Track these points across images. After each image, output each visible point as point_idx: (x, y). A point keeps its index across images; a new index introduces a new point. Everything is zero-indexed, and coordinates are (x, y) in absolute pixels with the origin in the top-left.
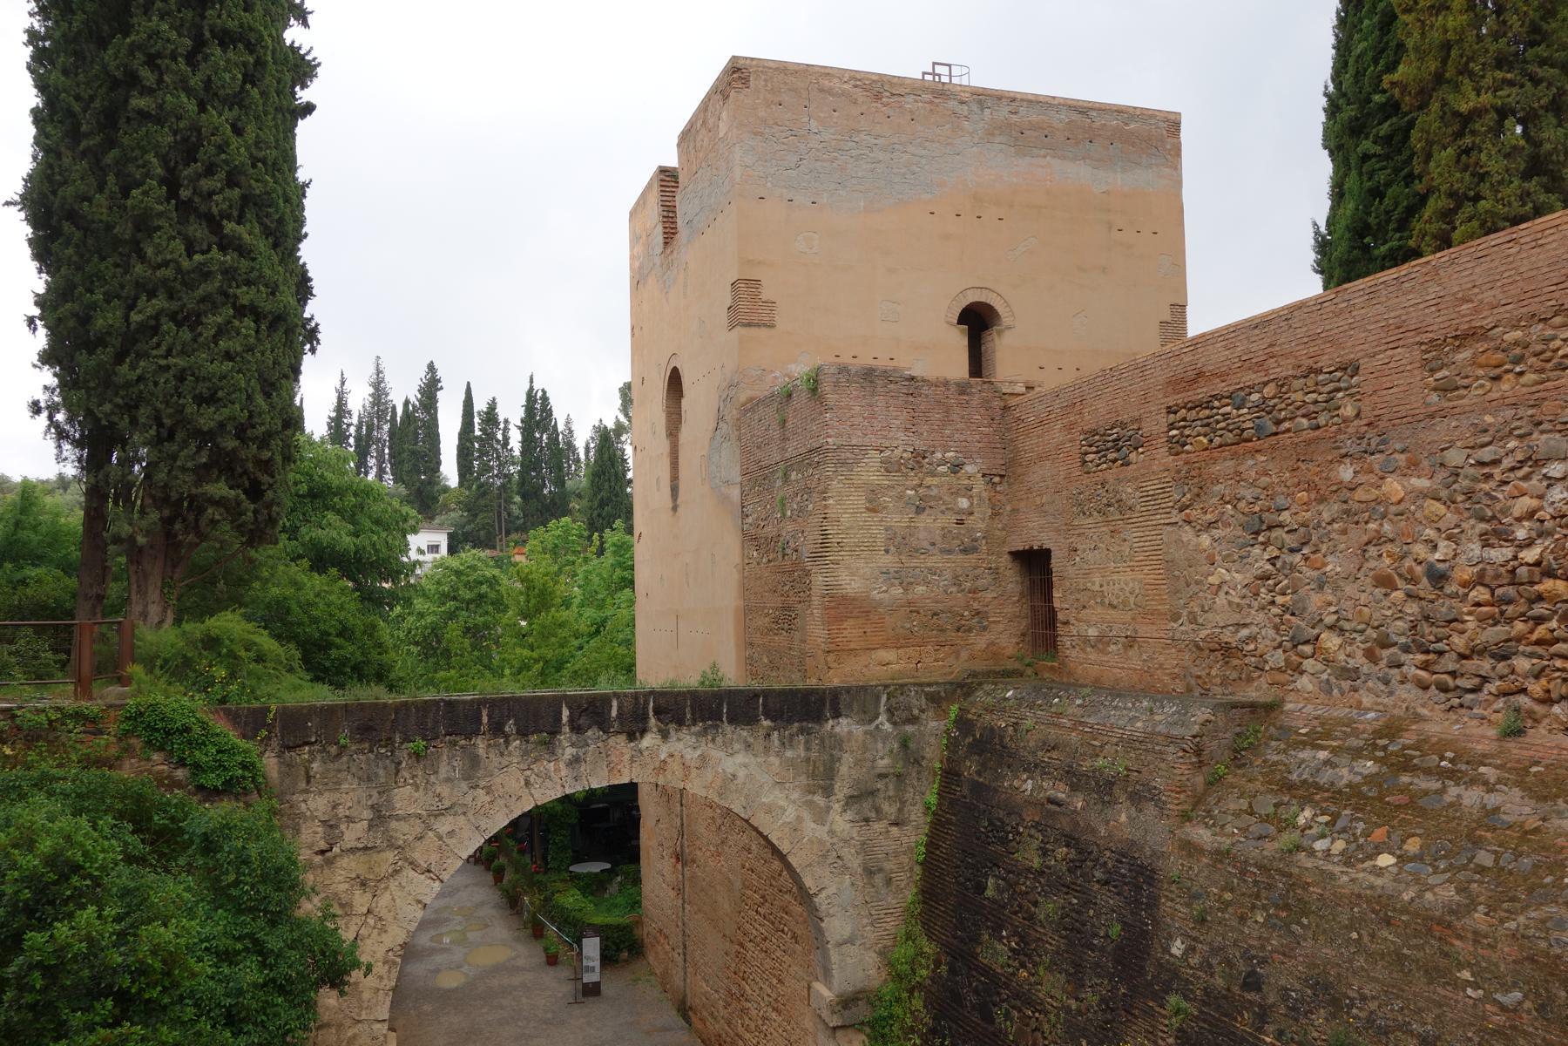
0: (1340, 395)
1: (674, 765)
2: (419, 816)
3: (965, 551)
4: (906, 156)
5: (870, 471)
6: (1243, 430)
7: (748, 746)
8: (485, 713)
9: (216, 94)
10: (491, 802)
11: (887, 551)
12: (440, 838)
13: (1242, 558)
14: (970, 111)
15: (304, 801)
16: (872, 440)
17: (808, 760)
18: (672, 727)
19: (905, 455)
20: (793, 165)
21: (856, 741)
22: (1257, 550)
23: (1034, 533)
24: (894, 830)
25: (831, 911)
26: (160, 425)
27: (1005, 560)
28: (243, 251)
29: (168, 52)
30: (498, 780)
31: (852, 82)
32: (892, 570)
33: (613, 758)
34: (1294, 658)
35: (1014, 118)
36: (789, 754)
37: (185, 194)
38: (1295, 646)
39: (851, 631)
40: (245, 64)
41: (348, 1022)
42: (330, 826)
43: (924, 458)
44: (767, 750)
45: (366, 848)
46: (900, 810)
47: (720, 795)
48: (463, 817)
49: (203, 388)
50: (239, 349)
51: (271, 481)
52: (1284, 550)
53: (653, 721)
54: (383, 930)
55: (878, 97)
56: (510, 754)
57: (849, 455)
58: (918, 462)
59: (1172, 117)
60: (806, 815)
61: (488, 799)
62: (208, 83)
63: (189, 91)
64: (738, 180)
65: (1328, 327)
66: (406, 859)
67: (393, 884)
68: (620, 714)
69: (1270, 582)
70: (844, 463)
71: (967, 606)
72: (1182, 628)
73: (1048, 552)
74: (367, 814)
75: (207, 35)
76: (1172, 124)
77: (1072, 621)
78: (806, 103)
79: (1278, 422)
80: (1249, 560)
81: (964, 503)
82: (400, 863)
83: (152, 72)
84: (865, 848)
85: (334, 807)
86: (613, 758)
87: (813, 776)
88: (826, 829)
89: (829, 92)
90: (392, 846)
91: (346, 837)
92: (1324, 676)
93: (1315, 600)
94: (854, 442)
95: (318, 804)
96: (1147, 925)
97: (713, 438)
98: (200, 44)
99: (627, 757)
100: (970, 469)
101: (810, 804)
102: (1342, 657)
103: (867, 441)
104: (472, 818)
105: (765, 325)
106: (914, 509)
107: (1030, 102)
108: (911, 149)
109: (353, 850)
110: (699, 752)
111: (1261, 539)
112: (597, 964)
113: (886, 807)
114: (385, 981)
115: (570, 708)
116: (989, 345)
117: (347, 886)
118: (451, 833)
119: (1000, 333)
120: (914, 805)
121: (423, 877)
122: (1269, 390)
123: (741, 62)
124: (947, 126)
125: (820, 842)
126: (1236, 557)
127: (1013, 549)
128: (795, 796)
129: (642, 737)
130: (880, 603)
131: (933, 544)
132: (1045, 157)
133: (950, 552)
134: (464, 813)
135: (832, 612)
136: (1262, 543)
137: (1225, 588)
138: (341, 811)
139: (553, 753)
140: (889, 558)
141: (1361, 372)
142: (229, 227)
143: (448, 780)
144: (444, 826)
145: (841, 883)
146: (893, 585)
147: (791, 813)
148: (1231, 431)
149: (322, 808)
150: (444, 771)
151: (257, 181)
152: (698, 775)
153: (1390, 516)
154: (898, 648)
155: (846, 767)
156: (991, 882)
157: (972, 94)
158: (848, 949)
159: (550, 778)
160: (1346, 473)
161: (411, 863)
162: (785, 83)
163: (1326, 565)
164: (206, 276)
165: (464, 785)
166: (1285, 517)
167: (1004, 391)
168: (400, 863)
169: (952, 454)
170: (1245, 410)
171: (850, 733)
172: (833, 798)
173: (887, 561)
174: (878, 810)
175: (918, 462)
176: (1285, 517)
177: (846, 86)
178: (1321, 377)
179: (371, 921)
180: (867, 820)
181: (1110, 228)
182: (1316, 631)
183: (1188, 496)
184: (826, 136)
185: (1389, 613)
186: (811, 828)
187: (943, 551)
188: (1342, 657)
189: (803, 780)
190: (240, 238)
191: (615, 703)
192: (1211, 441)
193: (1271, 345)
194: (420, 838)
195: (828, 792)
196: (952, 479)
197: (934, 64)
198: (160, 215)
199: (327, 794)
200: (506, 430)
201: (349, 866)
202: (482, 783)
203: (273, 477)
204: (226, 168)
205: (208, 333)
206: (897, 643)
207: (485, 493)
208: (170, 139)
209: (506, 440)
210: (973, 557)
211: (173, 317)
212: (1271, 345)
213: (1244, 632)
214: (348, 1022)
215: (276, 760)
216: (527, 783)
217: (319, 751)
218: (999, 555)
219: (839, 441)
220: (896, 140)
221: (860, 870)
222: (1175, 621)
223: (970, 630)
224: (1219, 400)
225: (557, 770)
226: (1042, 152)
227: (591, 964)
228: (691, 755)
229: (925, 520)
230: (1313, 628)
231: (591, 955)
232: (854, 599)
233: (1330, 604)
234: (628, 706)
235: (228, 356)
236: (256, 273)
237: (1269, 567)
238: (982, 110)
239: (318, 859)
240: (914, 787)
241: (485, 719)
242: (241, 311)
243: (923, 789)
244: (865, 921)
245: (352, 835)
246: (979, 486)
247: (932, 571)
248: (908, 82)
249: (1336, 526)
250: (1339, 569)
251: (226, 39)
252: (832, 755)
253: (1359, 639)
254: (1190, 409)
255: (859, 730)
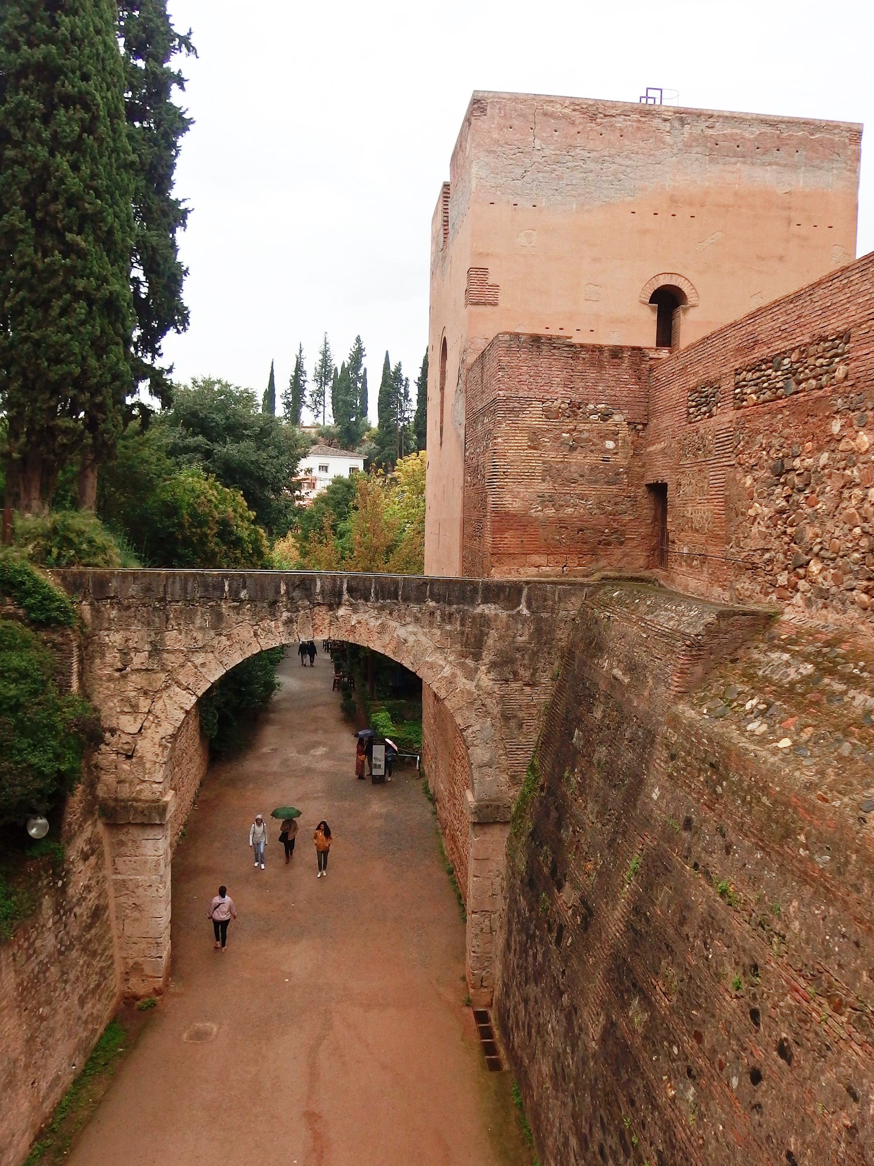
0: (837, 360)
1: (361, 630)
2: (181, 651)
3: (608, 483)
4: (614, 166)
5: (533, 418)
6: (778, 389)
7: (417, 620)
8: (227, 583)
9: (61, 143)
10: (230, 646)
11: (544, 480)
12: (196, 667)
13: (769, 495)
14: (672, 127)
15: (108, 635)
16: (536, 393)
17: (462, 633)
18: (362, 601)
19: (563, 406)
20: (519, 177)
21: (501, 622)
22: (778, 490)
23: (660, 472)
24: (527, 689)
25: (475, 742)
26: (26, 378)
27: (642, 491)
28: (82, 254)
29: (29, 116)
30: (235, 631)
31: (572, 107)
32: (546, 495)
33: (317, 621)
34: (793, 578)
35: (710, 132)
36: (448, 627)
37: (39, 215)
38: (795, 569)
39: (510, 539)
40: (82, 120)
41: (136, 781)
42: (125, 653)
43: (579, 408)
44: (431, 624)
45: (147, 670)
46: (533, 675)
47: (394, 653)
48: (211, 655)
49: (51, 353)
50: (74, 324)
51: (104, 417)
52: (795, 490)
53: (346, 596)
54: (158, 725)
55: (593, 118)
56: (243, 614)
57: (516, 405)
58: (573, 412)
59: (855, 128)
60: (459, 672)
61: (228, 643)
62: (55, 135)
63: (42, 142)
64: (473, 189)
65: (834, 301)
66: (173, 679)
67: (165, 695)
68: (322, 592)
69: (785, 516)
70: (512, 411)
71: (608, 525)
72: (732, 550)
73: (666, 485)
74: (147, 647)
75: (56, 100)
76: (855, 134)
77: (676, 541)
78: (533, 126)
79: (799, 383)
80: (773, 498)
81: (610, 444)
82: (170, 682)
83: (20, 130)
84: (503, 699)
85: (126, 641)
86: (317, 621)
87: (466, 644)
88: (474, 684)
89: (552, 115)
90: (164, 670)
91: (134, 662)
92: (809, 595)
93: (809, 532)
94: (520, 395)
95: (115, 638)
96: (644, 774)
97: (456, 391)
98: (51, 108)
99: (327, 621)
100: (617, 418)
101: (463, 665)
102: (820, 579)
103: (531, 395)
104: (217, 655)
105: (490, 304)
106: (568, 447)
107: (727, 117)
108: (618, 160)
109: (138, 670)
110: (380, 622)
111: (782, 480)
112: (382, 763)
113: (521, 672)
114: (160, 758)
115: (287, 584)
116: (676, 320)
117: (135, 693)
118: (203, 665)
119: (685, 310)
120: (545, 672)
121: (185, 692)
122: (795, 356)
123: (480, 94)
124: (651, 140)
125: (470, 693)
126: (765, 495)
127: (648, 482)
128: (451, 658)
129: (338, 608)
130: (537, 519)
131: (582, 476)
132: (735, 164)
133: (596, 482)
134: (212, 652)
135: (496, 524)
136: (782, 484)
137: (758, 520)
138: (131, 644)
139: (274, 615)
140: (544, 486)
141: (852, 340)
142: (69, 236)
143: (201, 628)
144: (199, 659)
145: (484, 723)
146: (547, 506)
147: (447, 671)
148: (770, 390)
149: (119, 641)
150: (198, 622)
151: (89, 203)
152: (379, 638)
153: (859, 465)
154: (548, 555)
155: (492, 640)
156: (577, 731)
157: (675, 113)
158: (486, 770)
159: (271, 632)
160: (836, 427)
161: (176, 682)
162: (515, 110)
163: (818, 503)
164: (54, 273)
165: (212, 633)
166: (797, 463)
167: (651, 356)
168: (170, 682)
169: (603, 406)
170: (779, 373)
171: (496, 615)
172: (480, 662)
173: (543, 487)
174: (515, 673)
175: (573, 412)
176: (797, 463)
177: (566, 111)
178: (827, 345)
179: (151, 718)
180: (507, 681)
181: (789, 223)
182: (808, 558)
183: (742, 443)
184: (547, 152)
185: (850, 545)
186: (462, 682)
187: (590, 482)
188: (820, 579)
189: (458, 647)
190: (78, 245)
191: (319, 583)
192: (758, 398)
193: (799, 317)
194: (182, 666)
195: (477, 657)
196: (603, 425)
197: (648, 89)
198: (23, 231)
199: (121, 632)
200: (406, 386)
201: (136, 680)
202: (225, 632)
203: (106, 414)
204: (66, 195)
205: (55, 312)
206: (550, 549)
207: (391, 432)
208: (29, 177)
209: (406, 395)
210: (614, 489)
211: (33, 304)
212: (799, 317)
213: (767, 556)
214: (136, 781)
215: (89, 607)
216: (256, 635)
217: (117, 603)
218: (638, 486)
219: (508, 393)
220: (606, 154)
221: (499, 716)
222: (728, 544)
223: (609, 544)
224: (765, 363)
225: (277, 627)
226: (733, 160)
227: (378, 763)
228: (374, 623)
229: (577, 457)
230: (807, 555)
231: (379, 757)
232: (515, 515)
233: (817, 536)
234: (328, 585)
235: (68, 329)
236: (88, 271)
237: (784, 503)
238: (683, 126)
239: (117, 674)
240: (545, 658)
241: (227, 588)
242: (77, 296)
243: (552, 661)
244: (501, 752)
245: (138, 660)
246: (625, 432)
247: (581, 497)
248: (620, 104)
249: (826, 471)
250: (824, 507)
251: (68, 101)
252: (481, 631)
253: (832, 565)
254: (749, 371)
255: (503, 614)
